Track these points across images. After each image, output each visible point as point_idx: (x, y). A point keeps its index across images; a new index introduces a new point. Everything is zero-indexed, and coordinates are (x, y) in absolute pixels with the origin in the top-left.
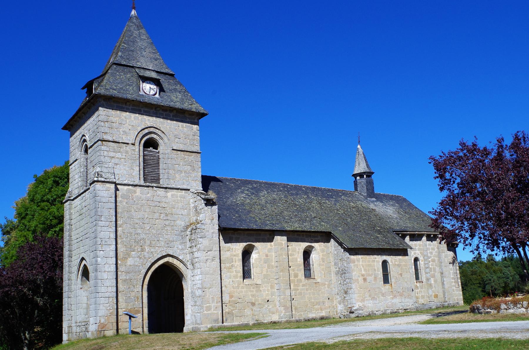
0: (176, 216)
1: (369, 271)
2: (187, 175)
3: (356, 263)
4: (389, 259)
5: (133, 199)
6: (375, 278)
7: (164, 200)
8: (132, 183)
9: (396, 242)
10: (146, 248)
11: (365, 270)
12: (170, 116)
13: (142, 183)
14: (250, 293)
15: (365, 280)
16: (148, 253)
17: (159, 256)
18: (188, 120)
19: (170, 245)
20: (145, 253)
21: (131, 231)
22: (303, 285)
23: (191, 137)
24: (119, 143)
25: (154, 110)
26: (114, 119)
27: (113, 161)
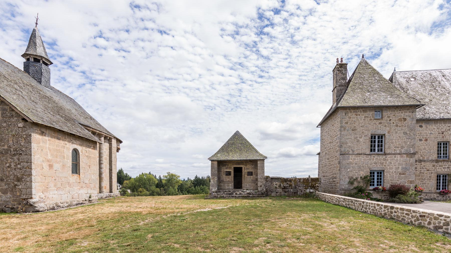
1: (57, 157)
3: (41, 144)
4: (79, 148)
6: (64, 166)
11: (52, 155)
15: (51, 166)
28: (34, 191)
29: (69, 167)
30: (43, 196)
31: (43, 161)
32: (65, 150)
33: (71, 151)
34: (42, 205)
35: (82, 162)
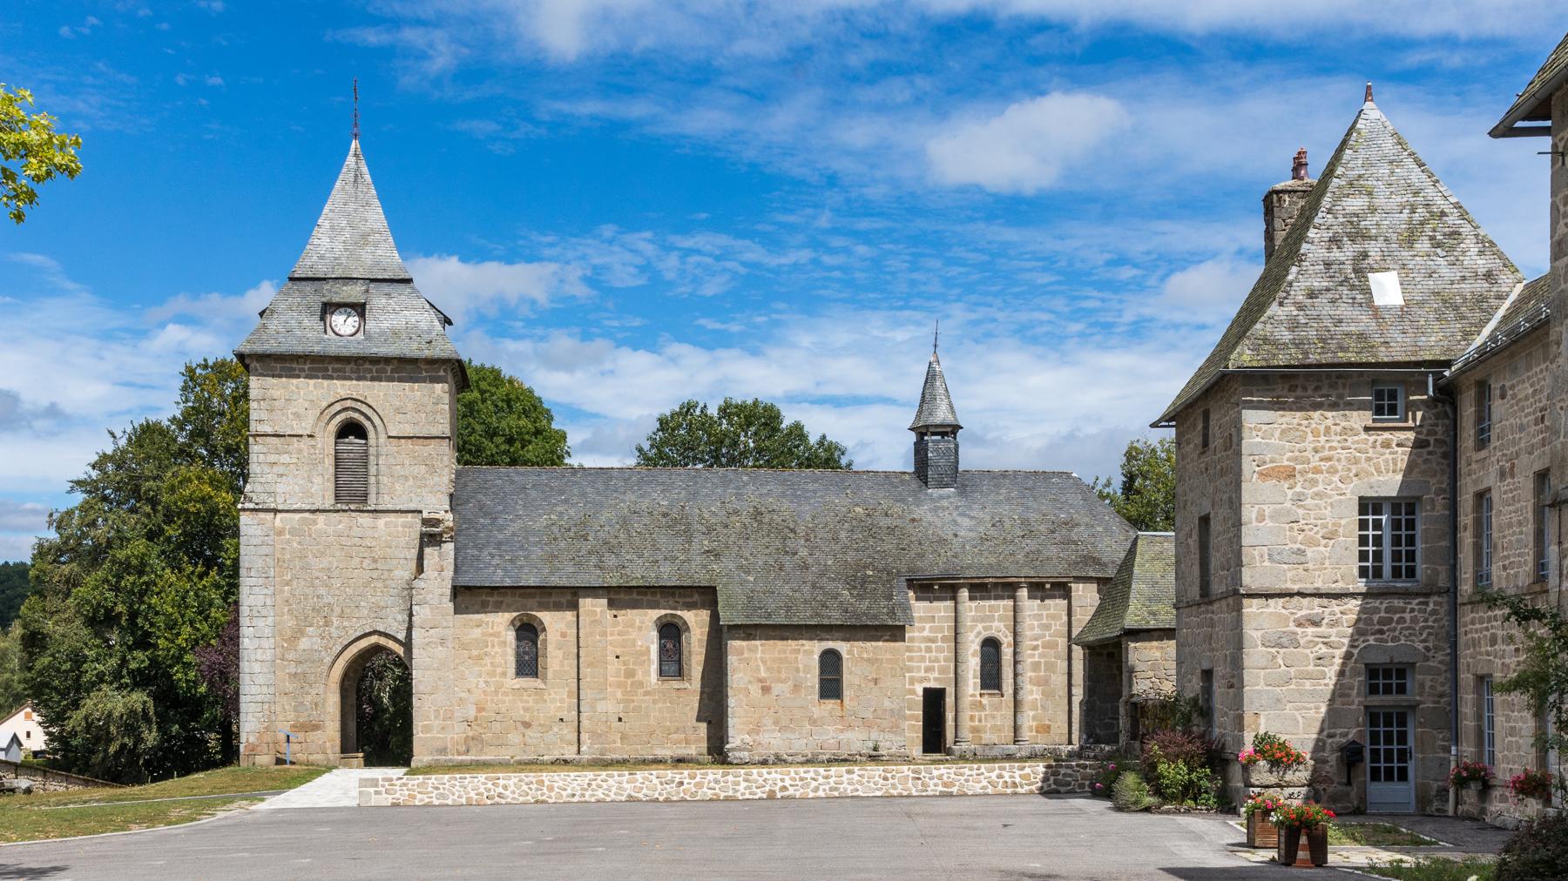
0: (394, 562)
4: (842, 647)
6: (797, 688)
7: (369, 533)
11: (768, 669)
13: (329, 502)
15: (766, 690)
21: (307, 591)
22: (647, 693)
23: (429, 408)
26: (276, 393)
27: (275, 469)
28: (731, 732)
30: (748, 739)
32: (800, 657)
33: (816, 657)
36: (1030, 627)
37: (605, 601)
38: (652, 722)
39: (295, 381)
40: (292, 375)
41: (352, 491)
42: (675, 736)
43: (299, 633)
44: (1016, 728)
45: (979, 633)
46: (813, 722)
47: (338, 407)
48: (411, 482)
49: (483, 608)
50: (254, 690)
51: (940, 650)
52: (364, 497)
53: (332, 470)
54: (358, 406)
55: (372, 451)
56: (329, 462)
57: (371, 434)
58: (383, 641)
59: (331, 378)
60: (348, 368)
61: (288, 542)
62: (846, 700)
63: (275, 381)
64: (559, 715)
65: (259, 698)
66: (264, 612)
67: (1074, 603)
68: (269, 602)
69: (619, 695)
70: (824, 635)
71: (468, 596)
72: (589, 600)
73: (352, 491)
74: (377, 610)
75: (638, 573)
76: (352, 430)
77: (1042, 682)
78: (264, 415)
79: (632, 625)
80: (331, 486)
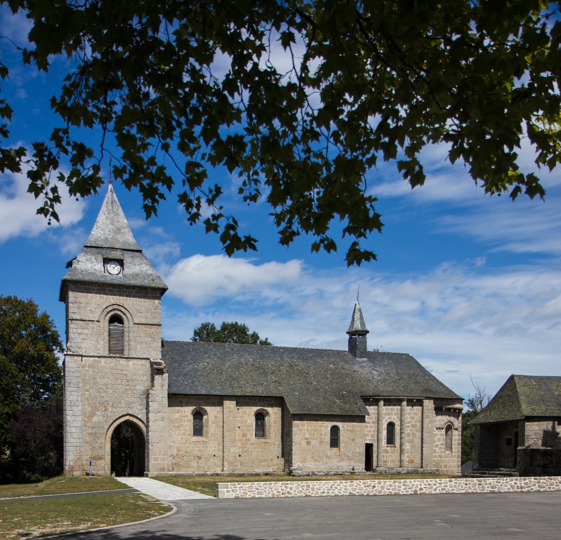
0: (137, 382)
1: (314, 435)
2: (148, 346)
3: (300, 427)
4: (340, 424)
5: (98, 368)
6: (321, 442)
7: (125, 368)
8: (97, 355)
9: (355, 408)
10: (109, 408)
11: (309, 434)
12: (132, 293)
13: (106, 353)
14: (197, 449)
15: (308, 443)
16: (111, 412)
17: (120, 415)
18: (150, 295)
19: (131, 406)
20: (108, 413)
21: (96, 394)
22: (252, 444)
23: (152, 311)
24: (85, 321)
25: (117, 289)
26: (82, 300)
27: (81, 336)
28: (294, 462)
29: (327, 442)
30: (300, 465)
31: (302, 440)
33: (329, 429)
34: (299, 472)
35: (343, 436)
36: (407, 418)
37: (235, 402)
38: (254, 457)
39: (90, 295)
40: (88, 291)
41: (116, 348)
42: (263, 463)
43: (93, 414)
44: (401, 461)
45: (387, 420)
46: (328, 458)
47: (110, 308)
48: (144, 345)
49: (181, 404)
50: (72, 440)
51: (371, 427)
52: (122, 351)
53: (107, 338)
54: (120, 308)
55: (126, 330)
56: (106, 334)
57: (126, 322)
58: (131, 418)
59: (107, 294)
60: (115, 290)
61: (88, 371)
62: (341, 448)
63: (81, 294)
64: (214, 454)
65: (75, 444)
66: (77, 404)
67: (424, 408)
68: (79, 399)
69: (240, 445)
70: (333, 419)
71: (175, 399)
72: (228, 402)
73: (116, 348)
74: (129, 404)
75: (248, 391)
76: (116, 319)
77: (411, 442)
78: (76, 310)
79: (245, 413)
80: (107, 345)
